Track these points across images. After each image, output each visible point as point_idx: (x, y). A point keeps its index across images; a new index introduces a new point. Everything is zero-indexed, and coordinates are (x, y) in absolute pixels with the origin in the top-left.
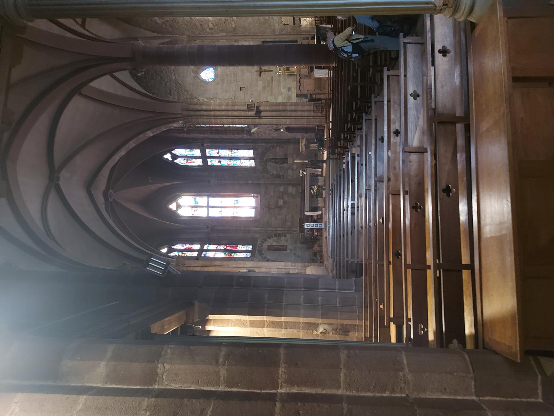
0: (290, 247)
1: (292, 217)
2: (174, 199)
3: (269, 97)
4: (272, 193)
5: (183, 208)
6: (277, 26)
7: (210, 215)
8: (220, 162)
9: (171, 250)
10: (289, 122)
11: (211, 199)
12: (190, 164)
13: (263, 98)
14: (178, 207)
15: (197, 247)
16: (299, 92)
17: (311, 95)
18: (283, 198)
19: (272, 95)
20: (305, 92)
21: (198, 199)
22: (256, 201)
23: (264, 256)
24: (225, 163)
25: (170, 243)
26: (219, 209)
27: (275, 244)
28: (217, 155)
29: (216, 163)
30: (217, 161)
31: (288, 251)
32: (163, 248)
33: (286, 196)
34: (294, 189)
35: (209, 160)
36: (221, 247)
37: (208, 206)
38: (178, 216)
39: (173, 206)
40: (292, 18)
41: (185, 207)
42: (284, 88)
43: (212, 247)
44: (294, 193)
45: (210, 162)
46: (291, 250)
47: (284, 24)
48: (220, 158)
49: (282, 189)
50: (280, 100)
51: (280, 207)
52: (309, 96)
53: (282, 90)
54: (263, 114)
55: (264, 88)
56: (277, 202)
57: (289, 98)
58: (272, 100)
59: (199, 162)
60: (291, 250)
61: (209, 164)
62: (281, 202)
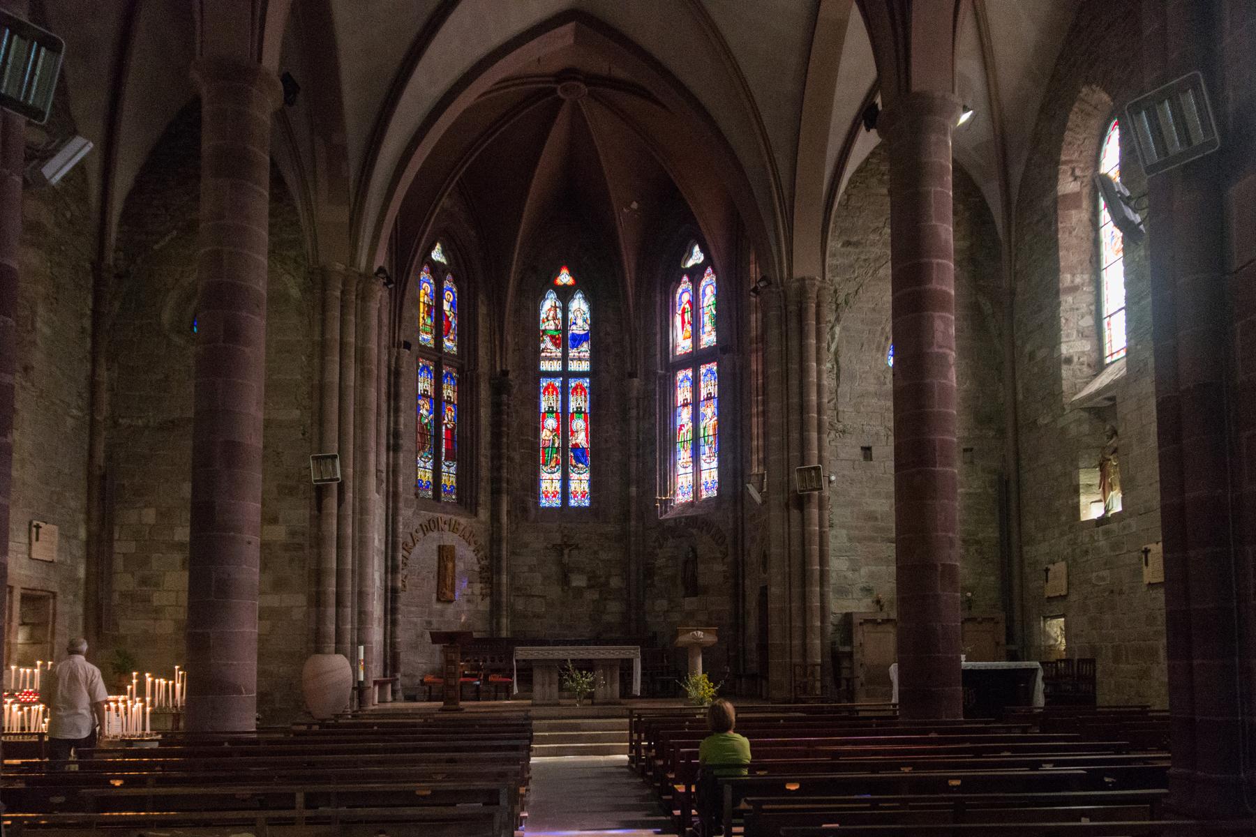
1: (538, 616)
2: (584, 284)
3: (844, 532)
6: (1044, 548)
7: (544, 383)
8: (685, 405)
10: (774, 590)
11: (586, 383)
12: (678, 319)
13: (839, 513)
14: (565, 295)
16: (856, 620)
17: (850, 655)
19: (850, 539)
20: (858, 638)
21: (585, 347)
24: (685, 416)
26: (557, 406)
28: (704, 393)
29: (683, 393)
30: (689, 396)
35: (689, 373)
36: (449, 415)
37: (566, 374)
39: (565, 278)
40: (1063, 593)
41: (565, 310)
42: (872, 575)
43: (449, 392)
45: (683, 375)
47: (1047, 570)
48: (695, 404)
50: (837, 565)
52: (847, 649)
53: (864, 571)
54: (795, 513)
55: (871, 517)
57: (843, 592)
58: (837, 538)
59: (682, 343)
61: (680, 375)
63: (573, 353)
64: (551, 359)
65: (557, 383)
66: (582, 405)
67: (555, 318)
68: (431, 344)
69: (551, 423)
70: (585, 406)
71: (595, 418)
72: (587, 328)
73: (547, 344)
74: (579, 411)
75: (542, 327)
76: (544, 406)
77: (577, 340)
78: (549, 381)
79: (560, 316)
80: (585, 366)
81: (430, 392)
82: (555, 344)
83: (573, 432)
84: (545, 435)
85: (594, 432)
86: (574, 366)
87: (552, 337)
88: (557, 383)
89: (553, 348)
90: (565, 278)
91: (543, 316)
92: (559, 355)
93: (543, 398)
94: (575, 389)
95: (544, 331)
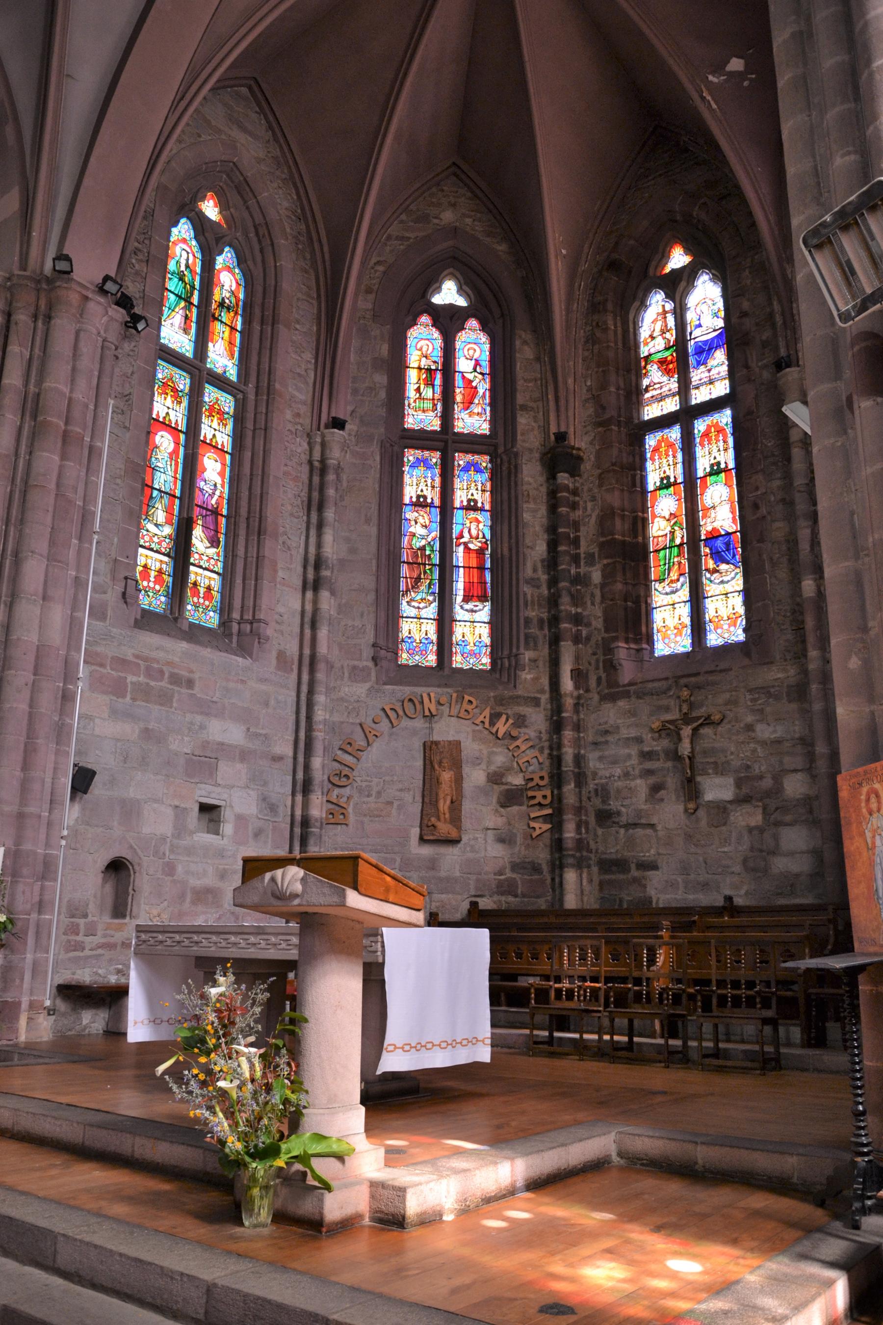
0: (451, 857)
4: (764, 732)
5: (669, 306)
9: (448, 322)
11: (725, 417)
15: (473, 421)
18: (742, 800)
22: (727, 649)
23: (385, 724)
25: (488, 309)
26: (677, 473)
27: (475, 777)
31: (427, 851)
32: (461, 291)
33: (757, 819)
34: (800, 865)
38: (630, 304)
44: (780, 864)
46: (432, 864)
49: (795, 786)
51: (691, 790)
56: (720, 769)
60: (432, 864)
62: (717, 789)
63: (697, 375)
64: (661, 398)
65: (675, 433)
66: (721, 458)
67: (663, 332)
68: (433, 423)
69: (666, 506)
70: (728, 458)
71: (745, 472)
72: (720, 323)
73: (654, 375)
74: (716, 470)
75: (644, 351)
76: (653, 479)
77: (705, 350)
78: (659, 435)
79: (671, 321)
80: (722, 389)
81: (433, 495)
82: (668, 372)
83: (706, 509)
84: (658, 528)
85: (747, 505)
86: (699, 396)
87: (662, 362)
88: (675, 433)
89: (665, 379)
90: (678, 259)
91: (644, 333)
92: (674, 386)
93: (649, 465)
94: (706, 435)
95: (646, 358)
